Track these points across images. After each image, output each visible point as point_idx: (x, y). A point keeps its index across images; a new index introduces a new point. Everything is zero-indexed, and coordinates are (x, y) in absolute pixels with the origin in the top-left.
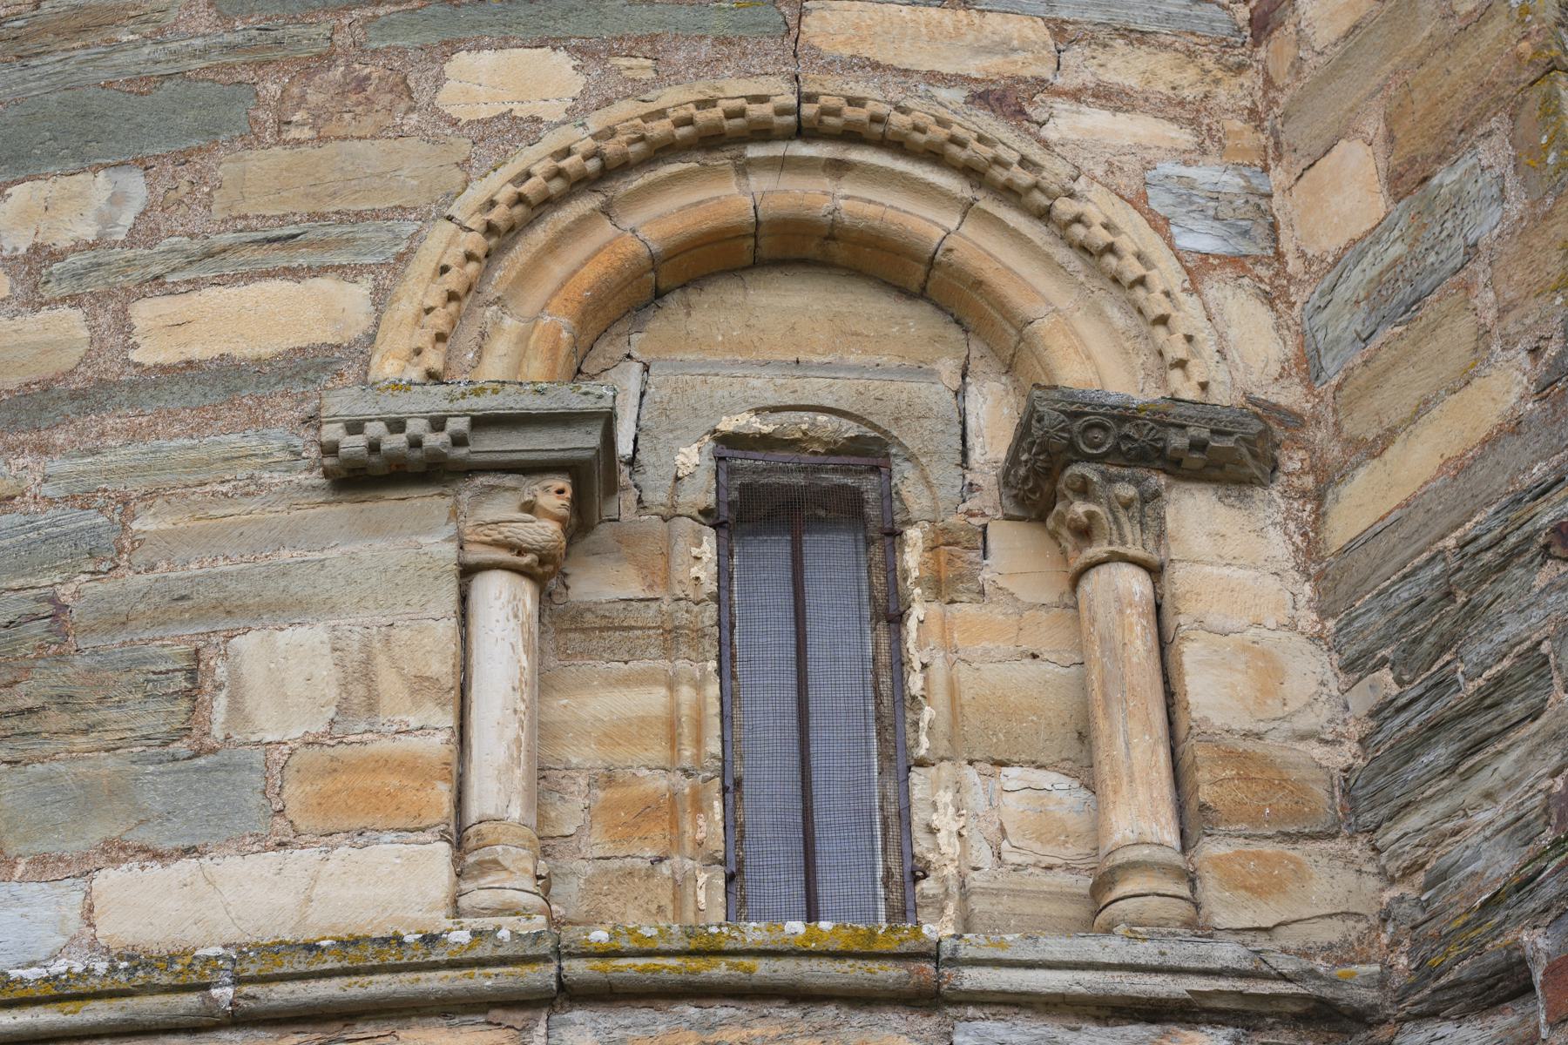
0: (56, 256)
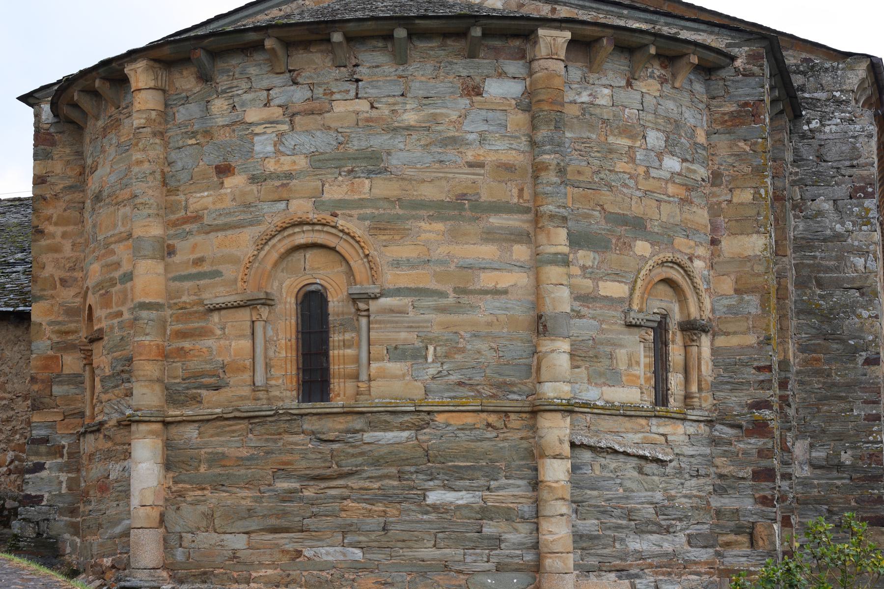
0: (587, 268)
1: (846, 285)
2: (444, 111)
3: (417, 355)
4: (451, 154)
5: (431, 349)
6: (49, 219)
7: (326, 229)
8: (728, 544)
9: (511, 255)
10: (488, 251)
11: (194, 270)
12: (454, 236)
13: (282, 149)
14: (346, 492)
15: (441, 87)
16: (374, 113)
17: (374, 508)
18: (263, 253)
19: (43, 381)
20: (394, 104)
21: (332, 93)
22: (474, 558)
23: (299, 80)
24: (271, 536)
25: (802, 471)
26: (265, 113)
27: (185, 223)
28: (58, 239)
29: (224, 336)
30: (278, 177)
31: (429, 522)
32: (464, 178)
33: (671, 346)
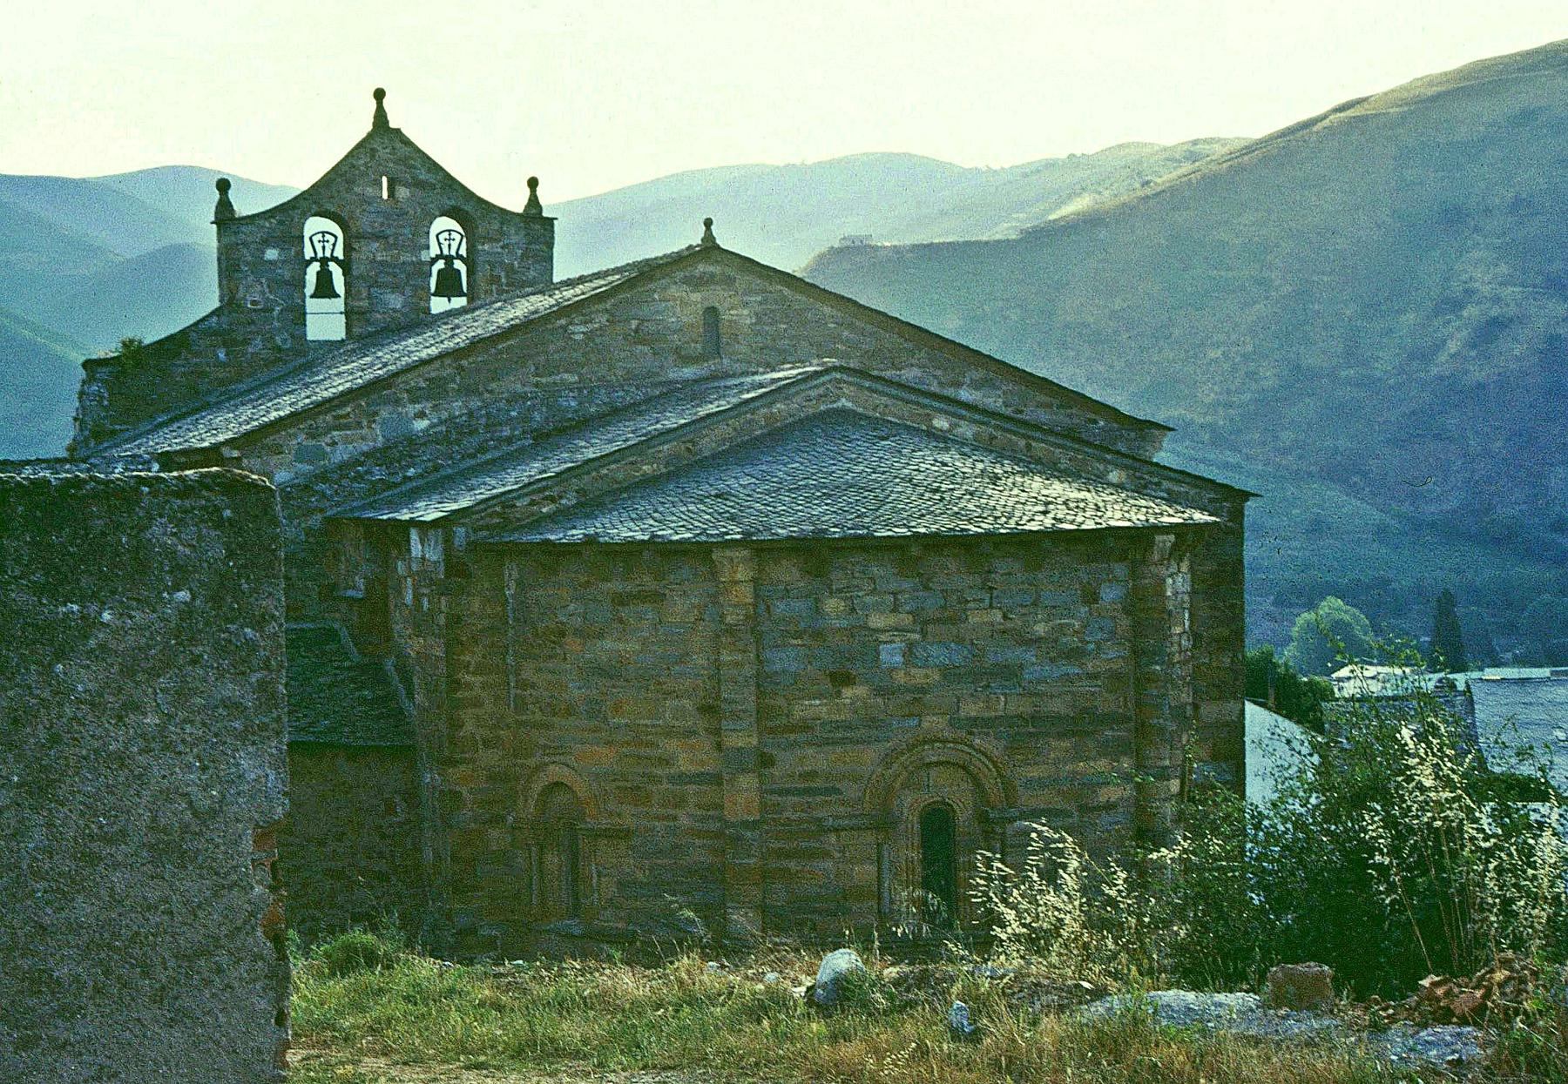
7: (960, 747)
16: (1009, 625)
26: (892, 620)
28: (477, 691)
30: (909, 690)
32: (1085, 687)
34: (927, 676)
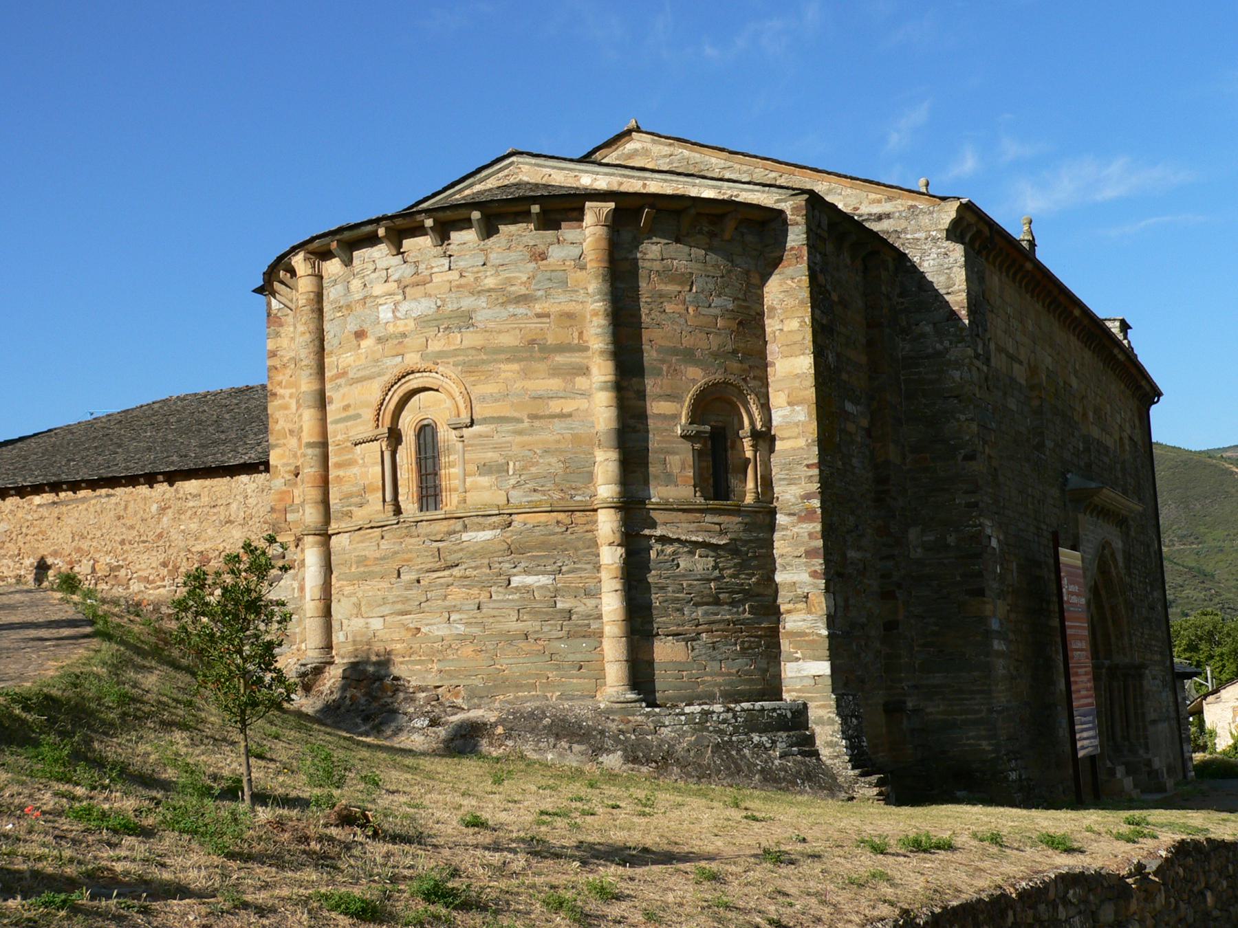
1: (946, 395)
2: (517, 274)
3: (500, 470)
4: (521, 310)
5: (511, 464)
6: (280, 384)
8: (789, 612)
9: (574, 386)
10: (555, 384)
11: (344, 415)
12: (526, 374)
13: (398, 314)
14: (450, 580)
15: (513, 255)
16: (463, 281)
17: (471, 592)
18: (387, 398)
19: (280, 511)
20: (477, 272)
21: (432, 267)
22: (549, 628)
23: (409, 259)
24: (400, 617)
25: (918, 553)
27: (337, 378)
29: (364, 465)
31: (512, 600)
32: (534, 325)
33: (730, 452)
34: (406, 325)
